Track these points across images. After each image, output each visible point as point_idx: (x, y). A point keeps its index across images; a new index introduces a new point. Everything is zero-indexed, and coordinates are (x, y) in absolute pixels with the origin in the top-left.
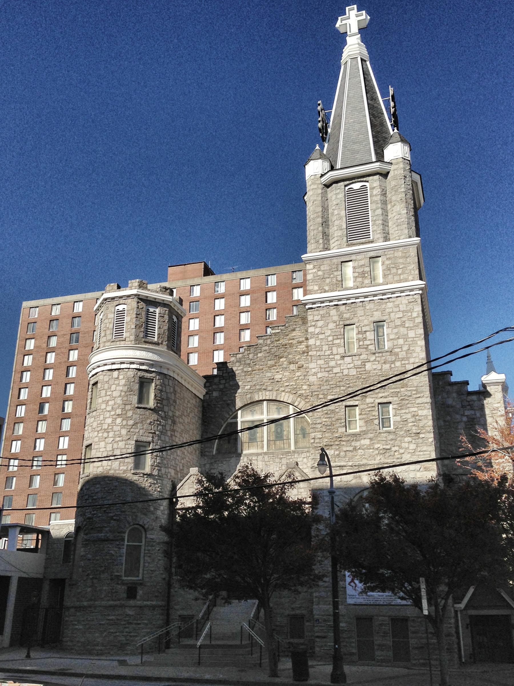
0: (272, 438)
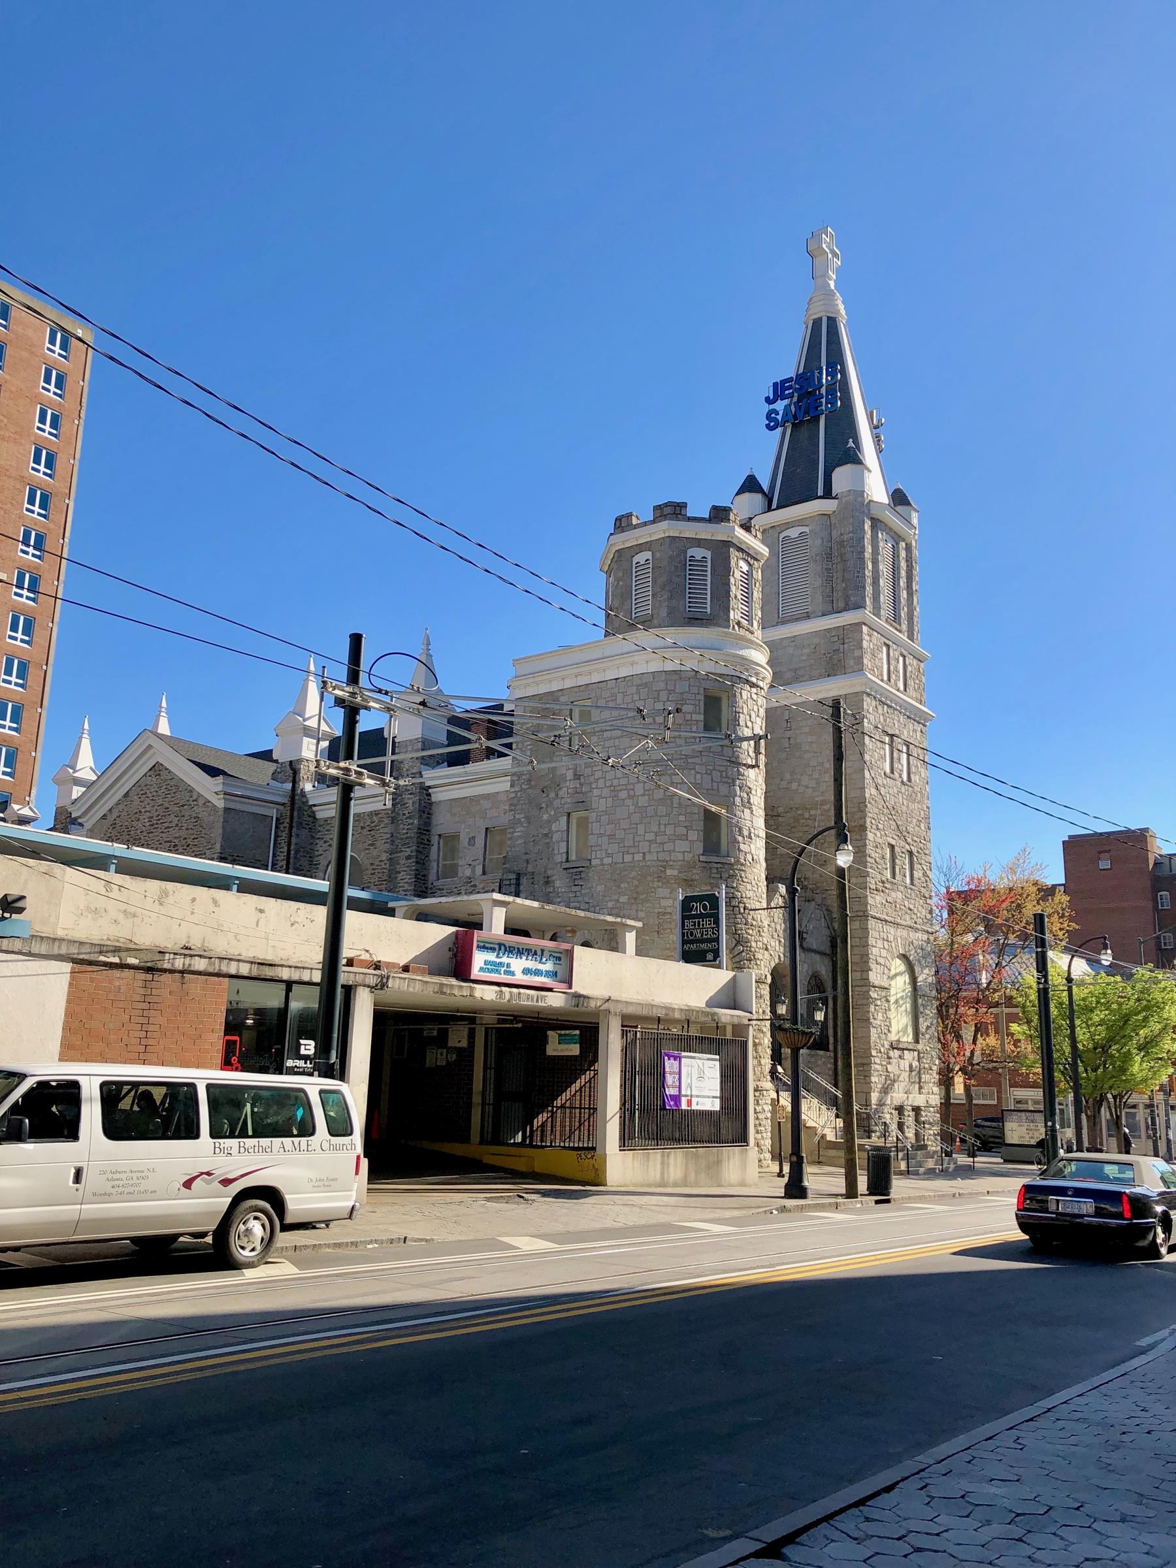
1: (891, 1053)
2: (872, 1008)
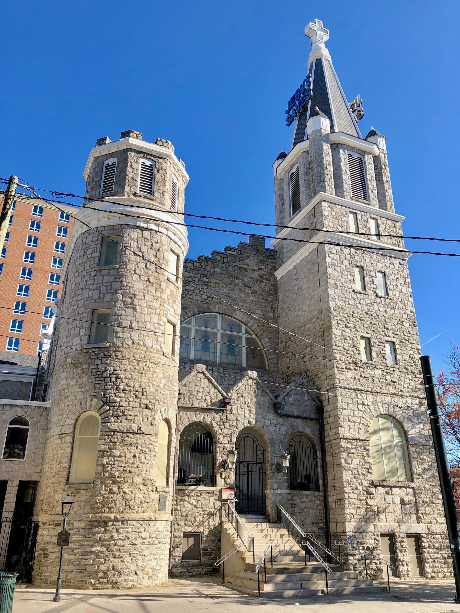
0: (225, 351)
1: (373, 490)
2: (344, 455)
